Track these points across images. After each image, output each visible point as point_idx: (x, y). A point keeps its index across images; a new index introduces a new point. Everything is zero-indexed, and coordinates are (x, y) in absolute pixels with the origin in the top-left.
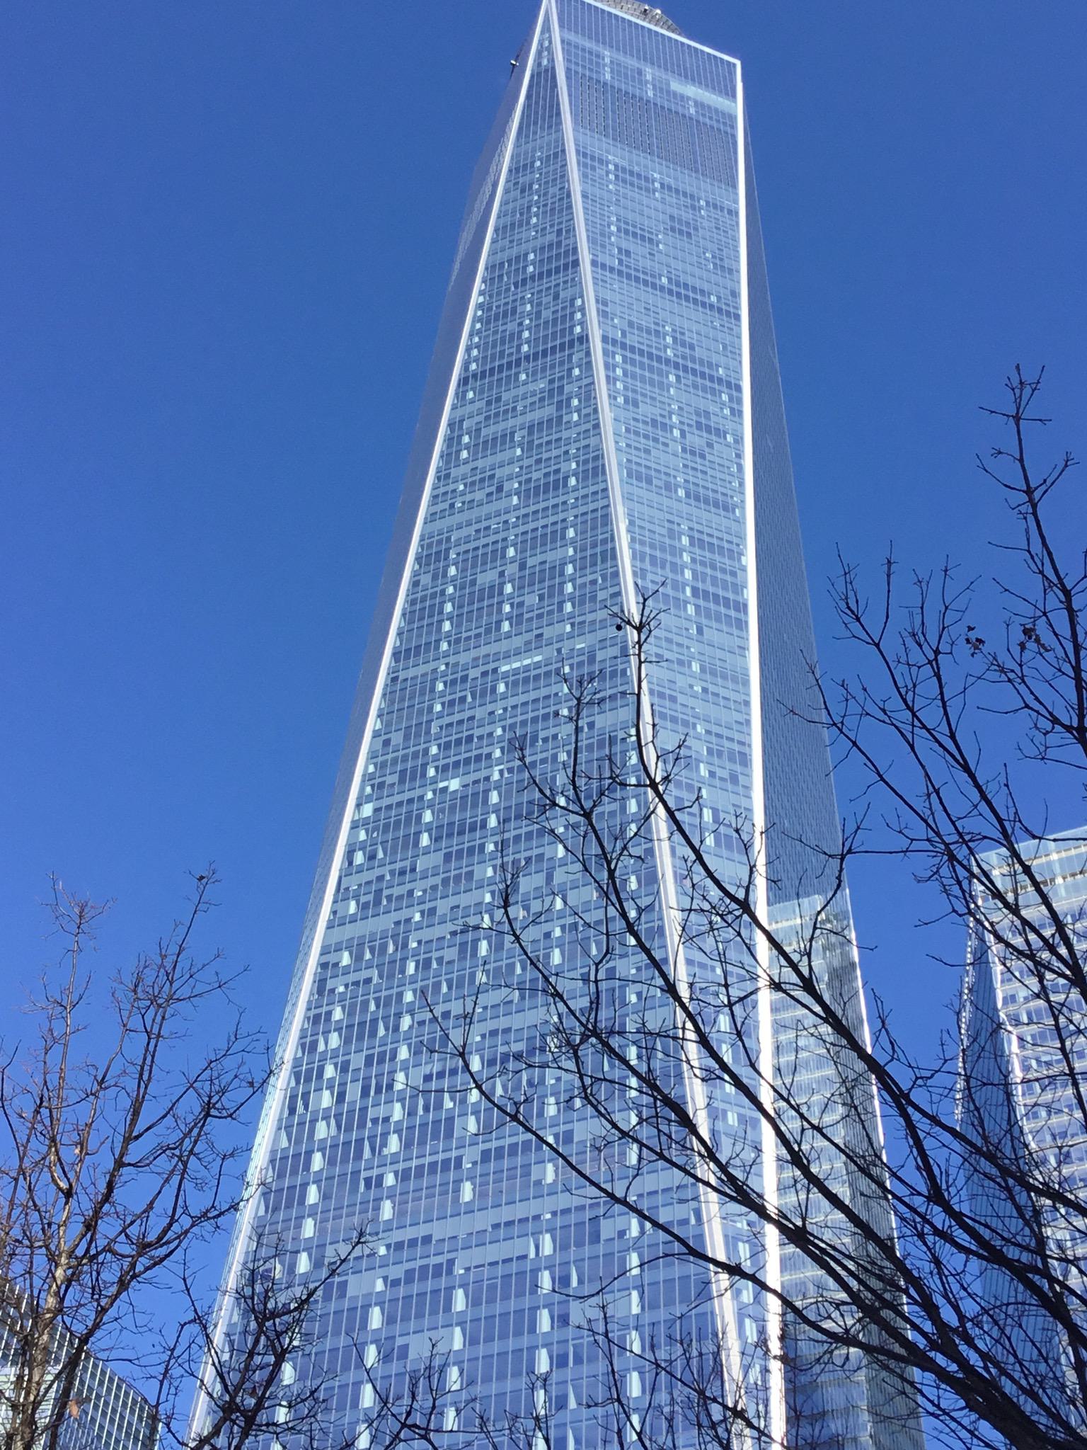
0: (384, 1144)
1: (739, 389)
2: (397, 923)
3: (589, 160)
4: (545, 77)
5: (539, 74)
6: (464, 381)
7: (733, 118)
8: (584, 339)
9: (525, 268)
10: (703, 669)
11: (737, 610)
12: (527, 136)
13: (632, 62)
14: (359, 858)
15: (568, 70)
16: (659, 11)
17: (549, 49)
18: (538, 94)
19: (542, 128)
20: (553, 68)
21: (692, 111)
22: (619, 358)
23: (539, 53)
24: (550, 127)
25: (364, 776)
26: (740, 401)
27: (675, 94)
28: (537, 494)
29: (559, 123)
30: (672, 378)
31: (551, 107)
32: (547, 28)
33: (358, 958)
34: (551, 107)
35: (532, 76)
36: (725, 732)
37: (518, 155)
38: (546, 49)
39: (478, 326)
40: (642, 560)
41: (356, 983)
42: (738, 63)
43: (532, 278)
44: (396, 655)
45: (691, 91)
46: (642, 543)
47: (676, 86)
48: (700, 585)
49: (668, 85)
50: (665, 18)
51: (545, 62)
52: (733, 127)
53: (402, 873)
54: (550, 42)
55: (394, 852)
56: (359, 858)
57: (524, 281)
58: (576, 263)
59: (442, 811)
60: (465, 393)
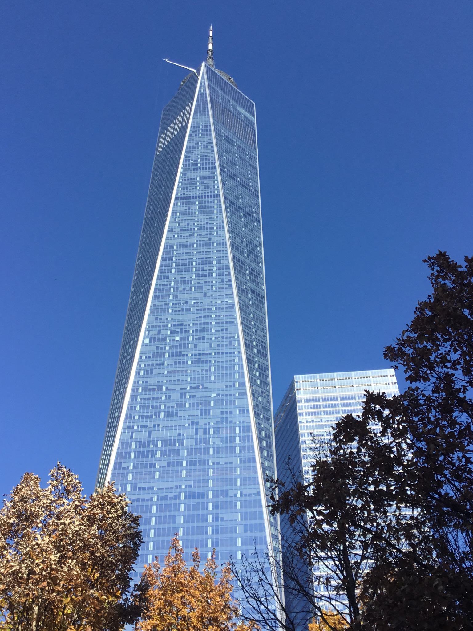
0: (156, 454)
1: (259, 222)
2: (158, 382)
3: (218, 132)
5: (201, 94)
6: (177, 198)
7: (254, 124)
8: (218, 196)
9: (197, 164)
10: (254, 316)
11: (262, 298)
12: (197, 116)
13: (227, 97)
15: (210, 96)
17: (204, 87)
18: (201, 101)
19: (202, 115)
20: (206, 94)
22: (228, 205)
23: (200, 87)
24: (205, 115)
26: (260, 225)
28: (203, 246)
29: (208, 115)
30: (242, 214)
31: (205, 108)
35: (198, 94)
36: (261, 339)
37: (194, 122)
41: (145, 399)
43: (200, 168)
44: (155, 290)
45: (242, 111)
51: (202, 91)
53: (160, 364)
54: (204, 84)
57: (197, 169)
58: (215, 168)
59: (173, 346)
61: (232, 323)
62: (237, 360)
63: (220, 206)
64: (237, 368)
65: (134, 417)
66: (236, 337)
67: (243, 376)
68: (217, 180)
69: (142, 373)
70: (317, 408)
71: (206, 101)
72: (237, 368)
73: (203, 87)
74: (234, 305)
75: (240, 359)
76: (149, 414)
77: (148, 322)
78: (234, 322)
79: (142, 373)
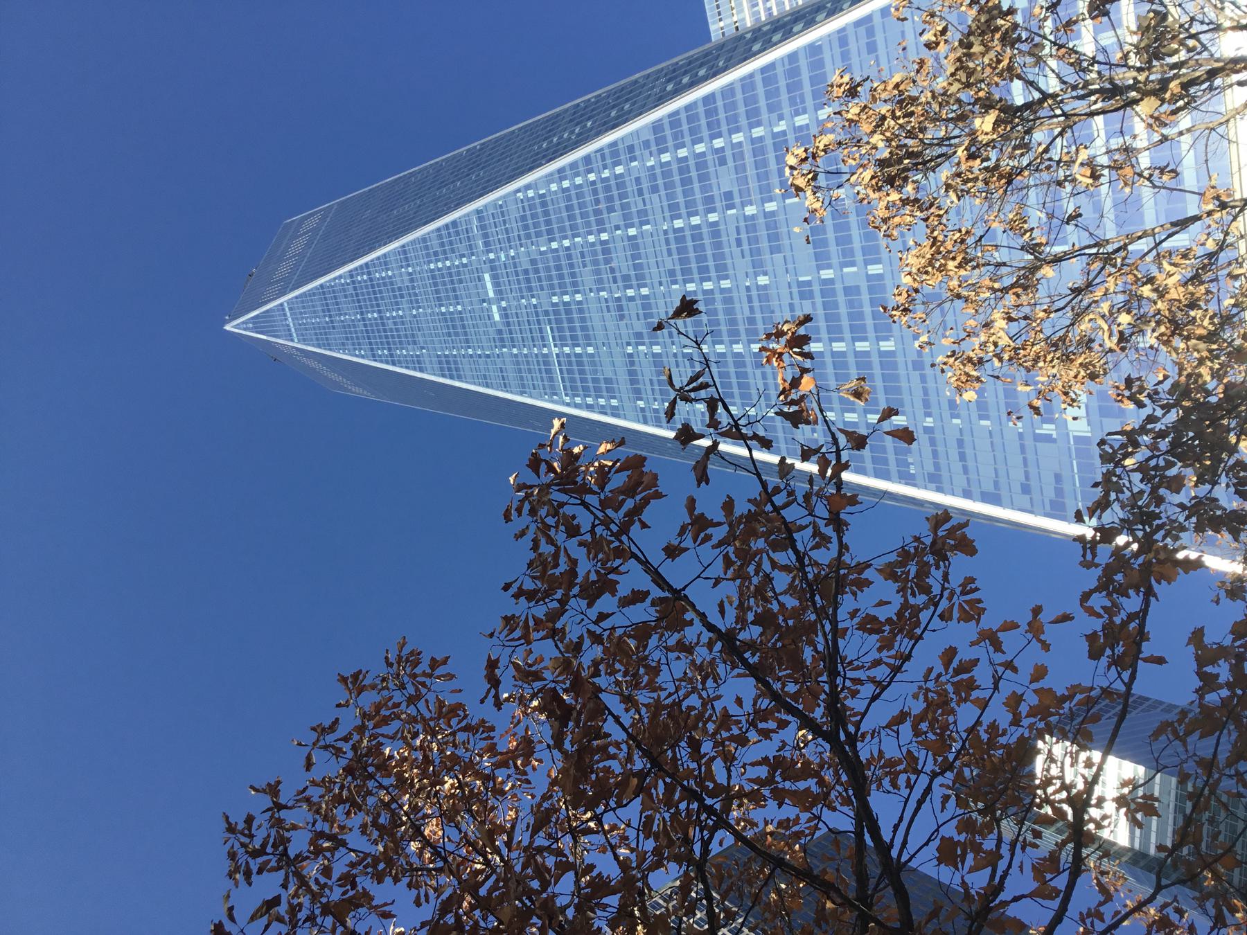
4: (257, 324)
8: (351, 274)
57: (332, 322)
58: (322, 286)
61: (501, 209)
62: (554, 187)
63: (361, 267)
64: (566, 184)
66: (520, 195)
67: (573, 165)
68: (335, 279)
69: (614, 402)
72: (566, 184)
75: (549, 179)
77: (540, 398)
78: (501, 206)
79: (614, 402)
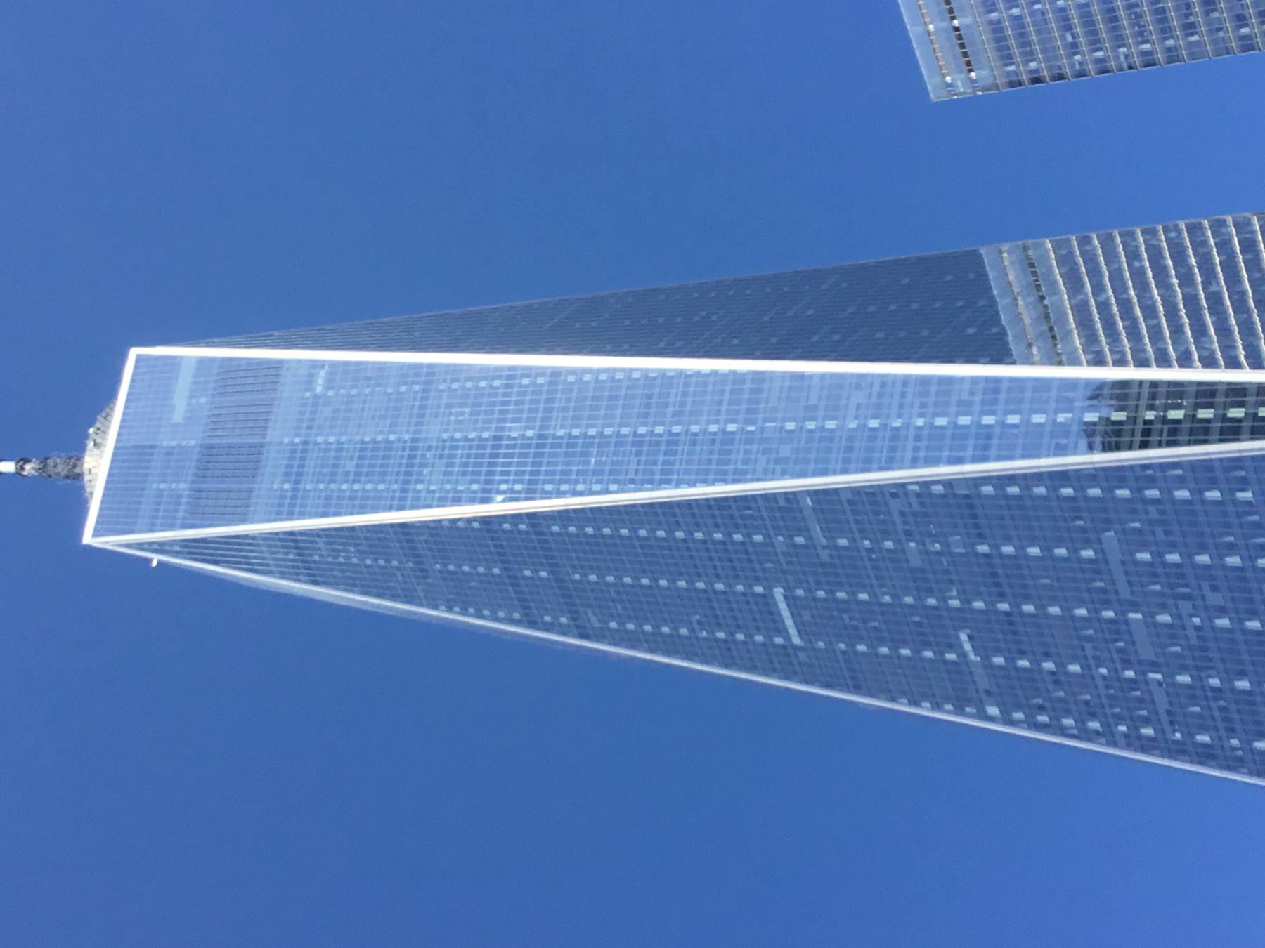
4: (192, 548)
6: (532, 624)
7: (202, 361)
14: (1043, 718)
16: (91, 430)
21: (203, 400)
25: (957, 714)
27: (186, 418)
32: (140, 546)
33: (1146, 721)
34: (226, 543)
37: (282, 573)
38: (161, 547)
39: (471, 610)
40: (725, 473)
42: (134, 352)
46: (707, 472)
47: (178, 417)
48: (741, 417)
49: (177, 425)
50: (98, 425)
51: (177, 548)
52: (212, 360)
55: (1037, 689)
56: (1043, 718)
60: (545, 623)
62: (988, 490)
65: (1234, 749)
70: (1022, 26)
71: (204, 540)
73: (167, 548)
74: (816, 492)
76: (1217, 714)
78: (868, 494)
